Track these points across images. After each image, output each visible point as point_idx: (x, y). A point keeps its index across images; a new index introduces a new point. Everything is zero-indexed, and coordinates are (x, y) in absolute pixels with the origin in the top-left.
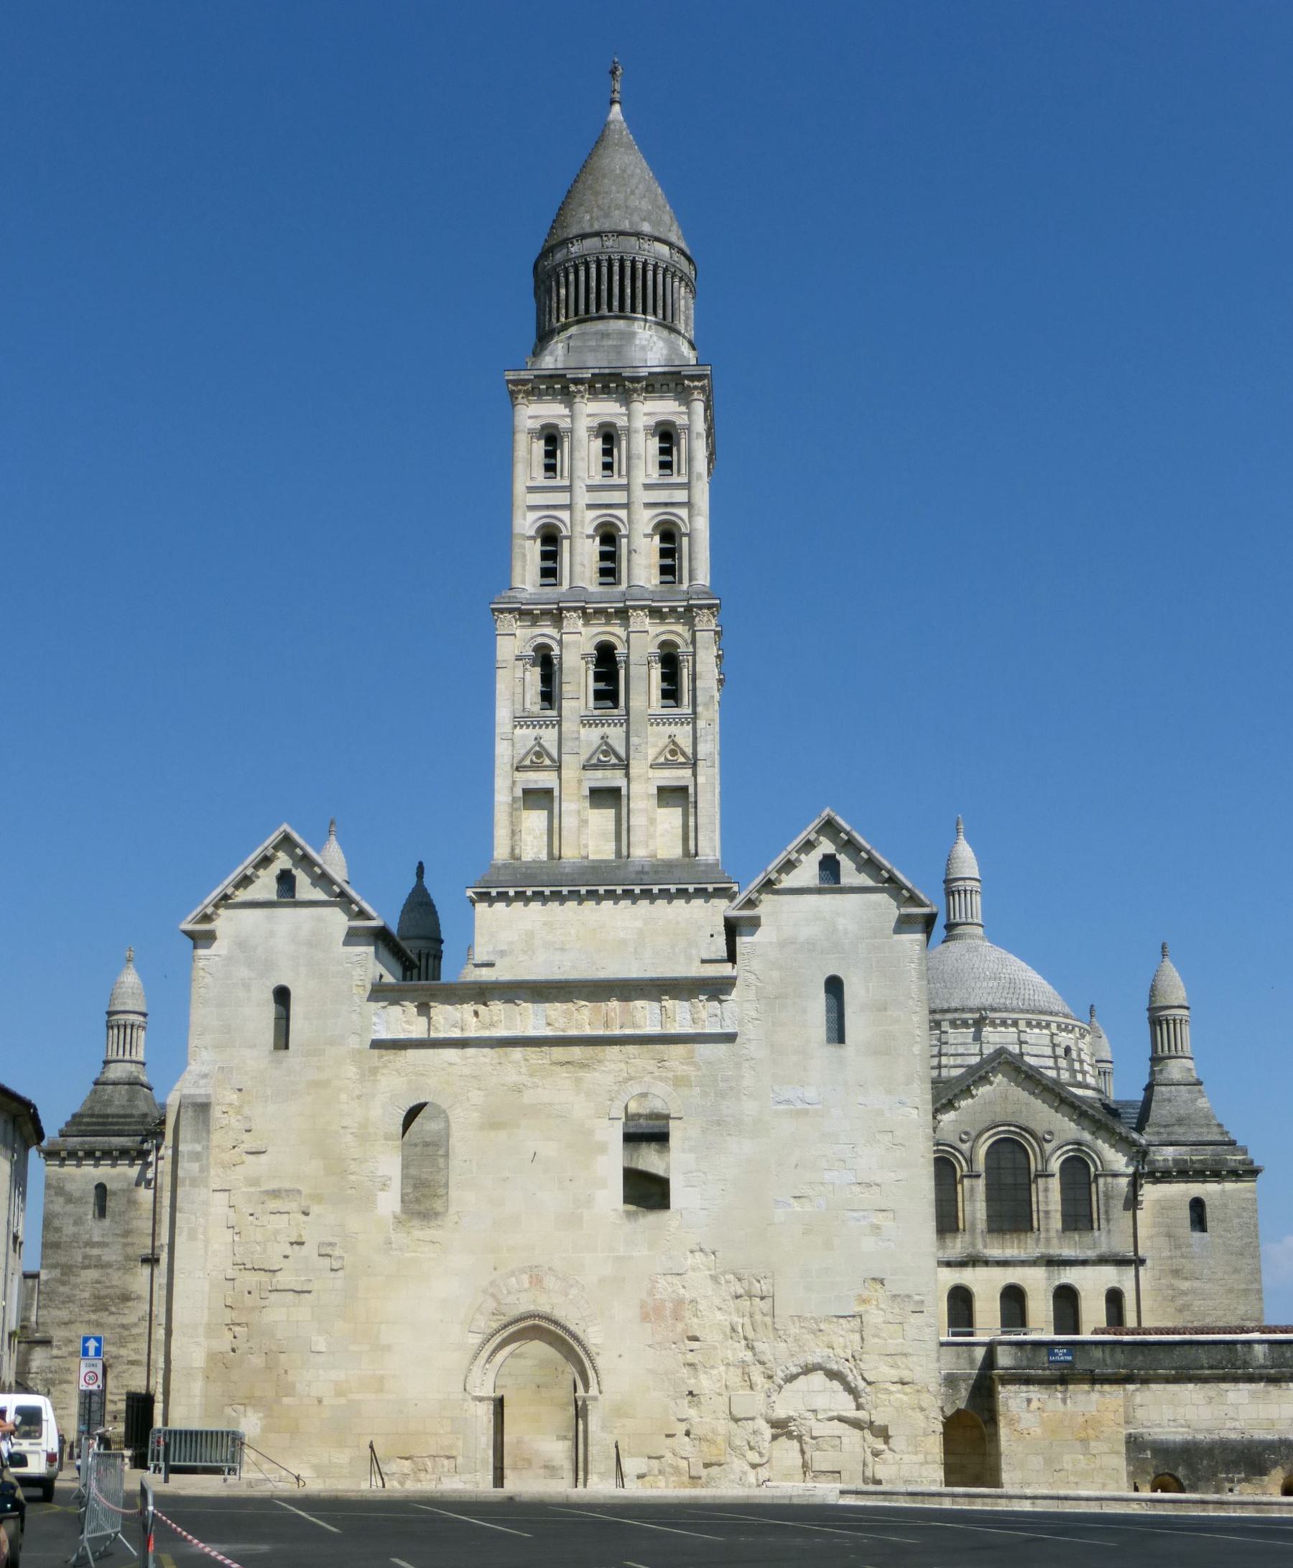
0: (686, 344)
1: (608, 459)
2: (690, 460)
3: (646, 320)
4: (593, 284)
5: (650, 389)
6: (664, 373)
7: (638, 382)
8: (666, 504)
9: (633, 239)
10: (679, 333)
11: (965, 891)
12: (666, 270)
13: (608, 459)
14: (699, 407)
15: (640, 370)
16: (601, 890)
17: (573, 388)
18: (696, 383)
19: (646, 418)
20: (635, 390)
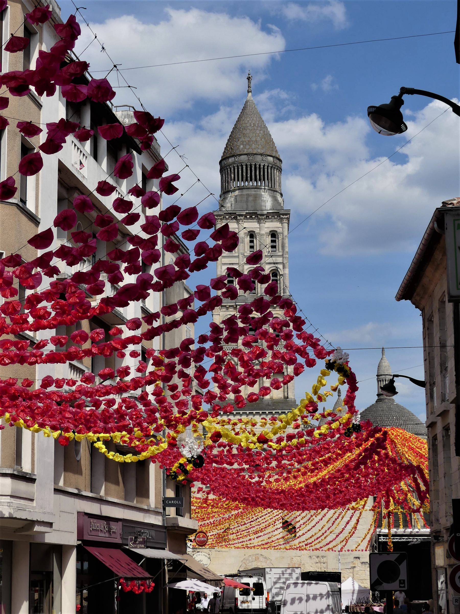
0: (279, 195)
1: (252, 244)
2: (283, 247)
3: (265, 189)
4: (244, 174)
5: (268, 218)
6: (273, 213)
7: (263, 216)
8: (274, 263)
9: (259, 156)
10: (277, 192)
11: (386, 380)
12: (271, 167)
13: (252, 244)
14: (286, 225)
15: (264, 211)
16: (254, 412)
17: (238, 218)
18: (285, 216)
19: (266, 229)
20: (262, 219)
